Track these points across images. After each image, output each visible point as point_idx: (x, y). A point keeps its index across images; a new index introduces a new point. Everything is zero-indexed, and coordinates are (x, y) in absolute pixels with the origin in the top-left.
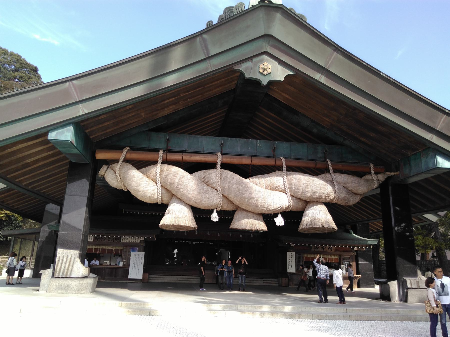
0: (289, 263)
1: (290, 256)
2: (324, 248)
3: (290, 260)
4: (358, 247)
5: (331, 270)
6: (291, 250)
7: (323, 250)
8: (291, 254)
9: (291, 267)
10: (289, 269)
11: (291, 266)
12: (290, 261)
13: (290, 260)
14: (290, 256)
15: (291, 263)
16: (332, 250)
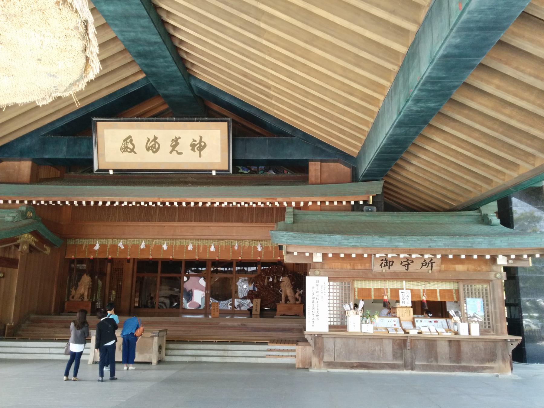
0: (311, 307)
1: (313, 287)
2: (409, 264)
3: (313, 298)
4: (508, 256)
5: (436, 322)
6: (318, 273)
7: (407, 270)
8: (317, 282)
9: (315, 318)
10: (311, 321)
11: (316, 314)
12: (315, 300)
13: (313, 298)
14: (313, 287)
15: (315, 307)
16: (433, 268)
